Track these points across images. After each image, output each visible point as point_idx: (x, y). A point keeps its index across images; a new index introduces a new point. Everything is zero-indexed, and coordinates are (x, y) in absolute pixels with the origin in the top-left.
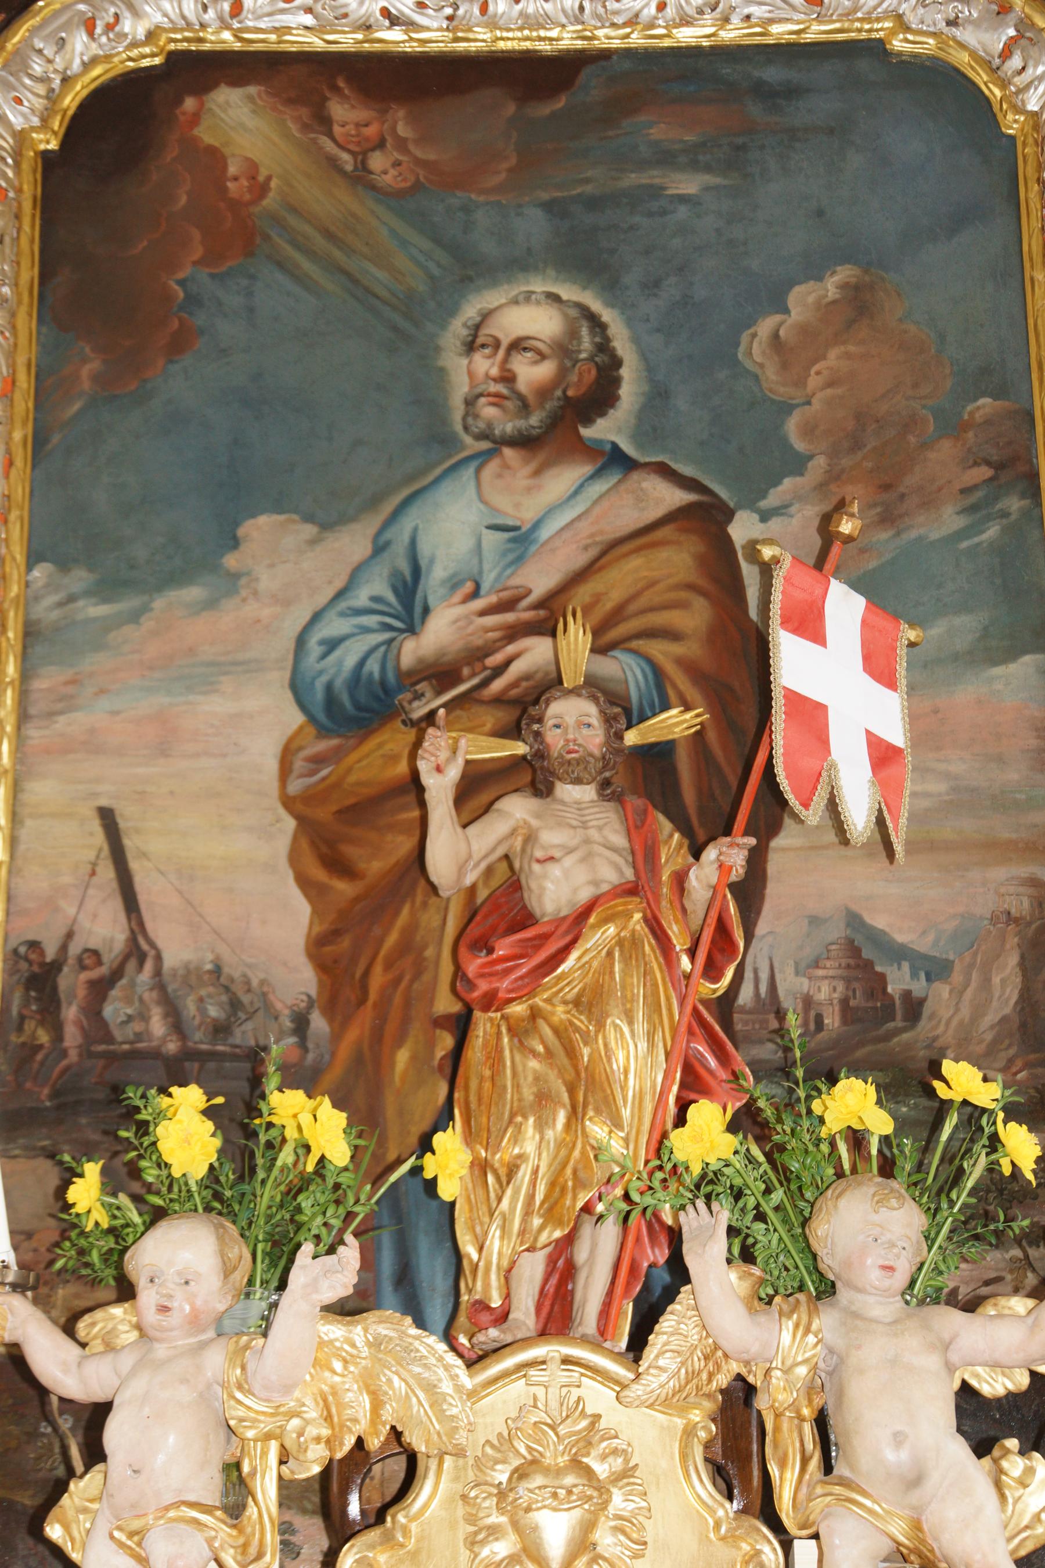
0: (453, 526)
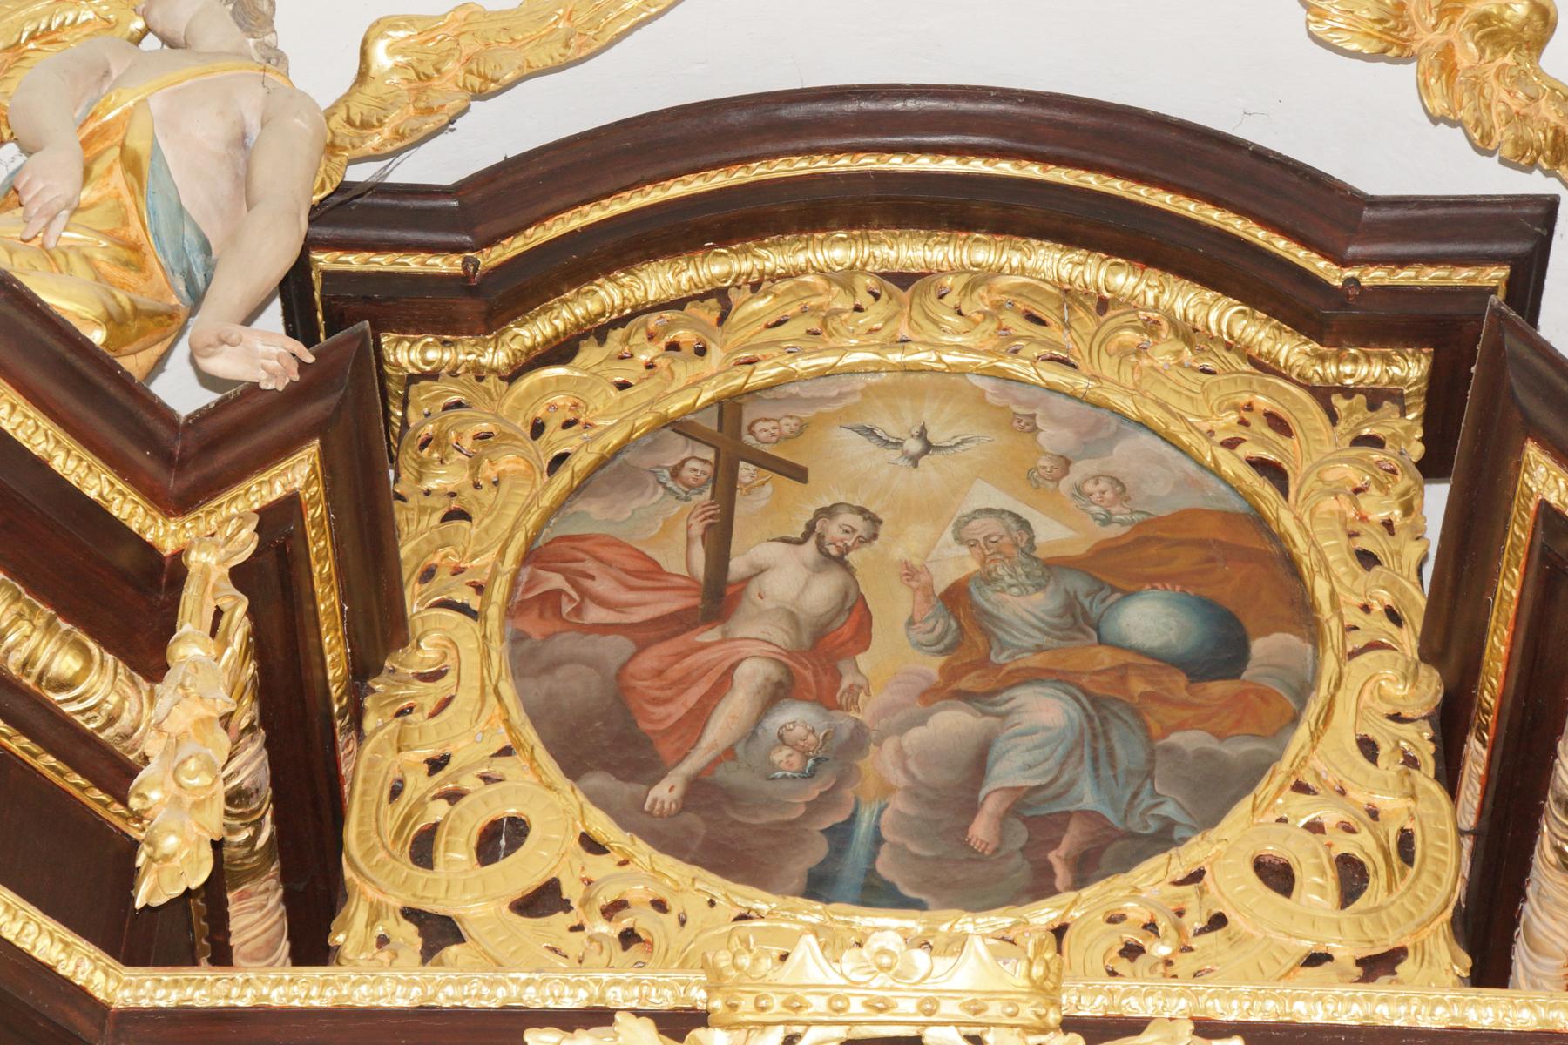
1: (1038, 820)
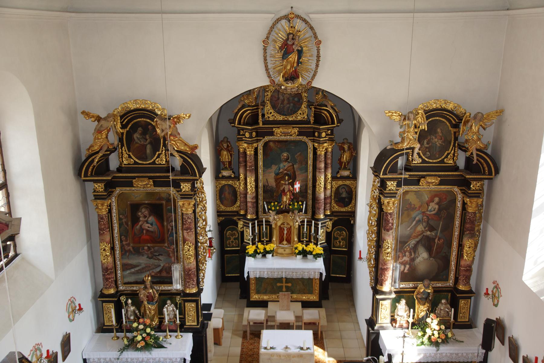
0: (281, 165)
1: (291, 110)
